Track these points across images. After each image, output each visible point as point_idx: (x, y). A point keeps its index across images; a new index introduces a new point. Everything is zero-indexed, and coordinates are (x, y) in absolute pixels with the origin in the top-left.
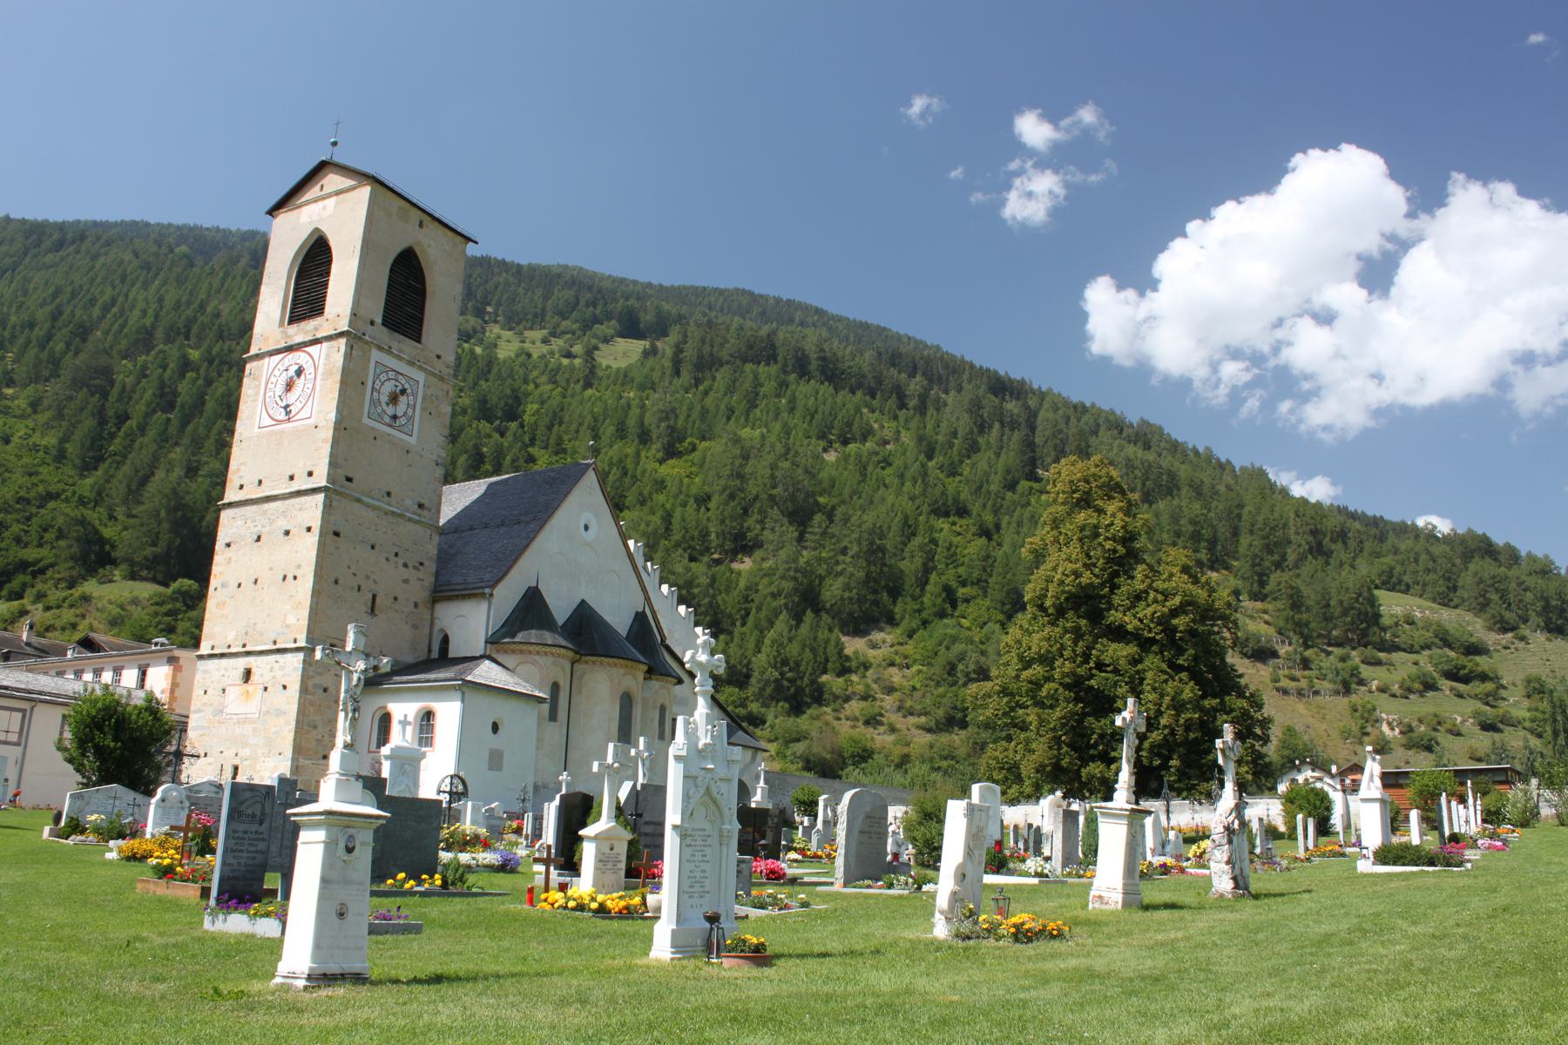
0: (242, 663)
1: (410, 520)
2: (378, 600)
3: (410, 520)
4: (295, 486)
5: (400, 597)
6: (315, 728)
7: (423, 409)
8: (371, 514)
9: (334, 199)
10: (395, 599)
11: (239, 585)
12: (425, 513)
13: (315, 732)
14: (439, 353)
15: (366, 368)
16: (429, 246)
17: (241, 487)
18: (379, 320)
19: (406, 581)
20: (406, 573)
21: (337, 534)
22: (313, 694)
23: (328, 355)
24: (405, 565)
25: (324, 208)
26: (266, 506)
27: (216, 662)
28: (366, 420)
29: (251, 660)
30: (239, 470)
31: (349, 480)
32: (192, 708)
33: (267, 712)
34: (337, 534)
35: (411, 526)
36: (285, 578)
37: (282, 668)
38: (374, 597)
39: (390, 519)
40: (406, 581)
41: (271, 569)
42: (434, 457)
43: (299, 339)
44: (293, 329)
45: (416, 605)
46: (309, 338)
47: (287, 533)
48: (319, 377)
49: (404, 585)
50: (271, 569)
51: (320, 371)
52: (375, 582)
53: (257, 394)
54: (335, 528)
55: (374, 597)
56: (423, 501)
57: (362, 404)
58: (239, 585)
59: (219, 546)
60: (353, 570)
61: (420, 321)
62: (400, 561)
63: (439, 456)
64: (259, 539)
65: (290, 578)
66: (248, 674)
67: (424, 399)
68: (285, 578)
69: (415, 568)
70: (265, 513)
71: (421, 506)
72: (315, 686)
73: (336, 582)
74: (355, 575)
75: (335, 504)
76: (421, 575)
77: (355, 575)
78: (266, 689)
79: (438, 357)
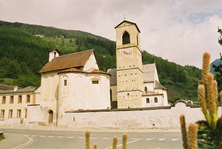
0: (127, 93)
4: (131, 68)
9: (128, 26)
11: (123, 82)
17: (120, 68)
23: (133, 49)
25: (126, 28)
26: (126, 70)
27: (121, 92)
29: (129, 92)
30: (119, 65)
32: (118, 99)
33: (133, 99)
36: (133, 80)
37: (135, 93)
41: (129, 79)
43: (126, 47)
44: (124, 45)
46: (129, 46)
47: (132, 74)
48: (132, 52)
50: (129, 79)
51: (132, 51)
53: (120, 54)
58: (123, 82)
59: (118, 76)
64: (126, 75)
65: (134, 80)
66: (128, 94)
68: (133, 80)
70: (126, 71)
78: (133, 96)
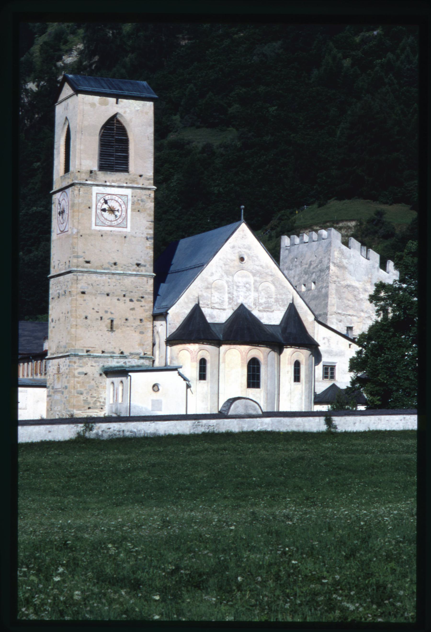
1: (131, 275)
2: (115, 323)
3: (131, 275)
5: (129, 319)
6: (82, 394)
7: (133, 210)
8: (104, 277)
10: (126, 320)
12: (142, 268)
13: (82, 396)
14: (141, 173)
15: (90, 200)
16: (125, 112)
18: (95, 168)
19: (133, 309)
20: (132, 305)
21: (83, 293)
22: (78, 377)
24: (131, 300)
28: (94, 227)
31: (88, 262)
34: (83, 293)
35: (133, 278)
38: (112, 321)
39: (118, 277)
40: (133, 309)
42: (145, 235)
45: (141, 320)
49: (132, 312)
52: (112, 313)
54: (82, 290)
55: (112, 321)
56: (139, 262)
57: (90, 219)
60: (96, 309)
61: (126, 158)
62: (127, 299)
63: (148, 234)
67: (133, 204)
69: (138, 300)
71: (138, 265)
72: (79, 373)
73: (86, 318)
74: (98, 312)
75: (80, 278)
76: (143, 303)
77: (98, 312)
79: (141, 176)
